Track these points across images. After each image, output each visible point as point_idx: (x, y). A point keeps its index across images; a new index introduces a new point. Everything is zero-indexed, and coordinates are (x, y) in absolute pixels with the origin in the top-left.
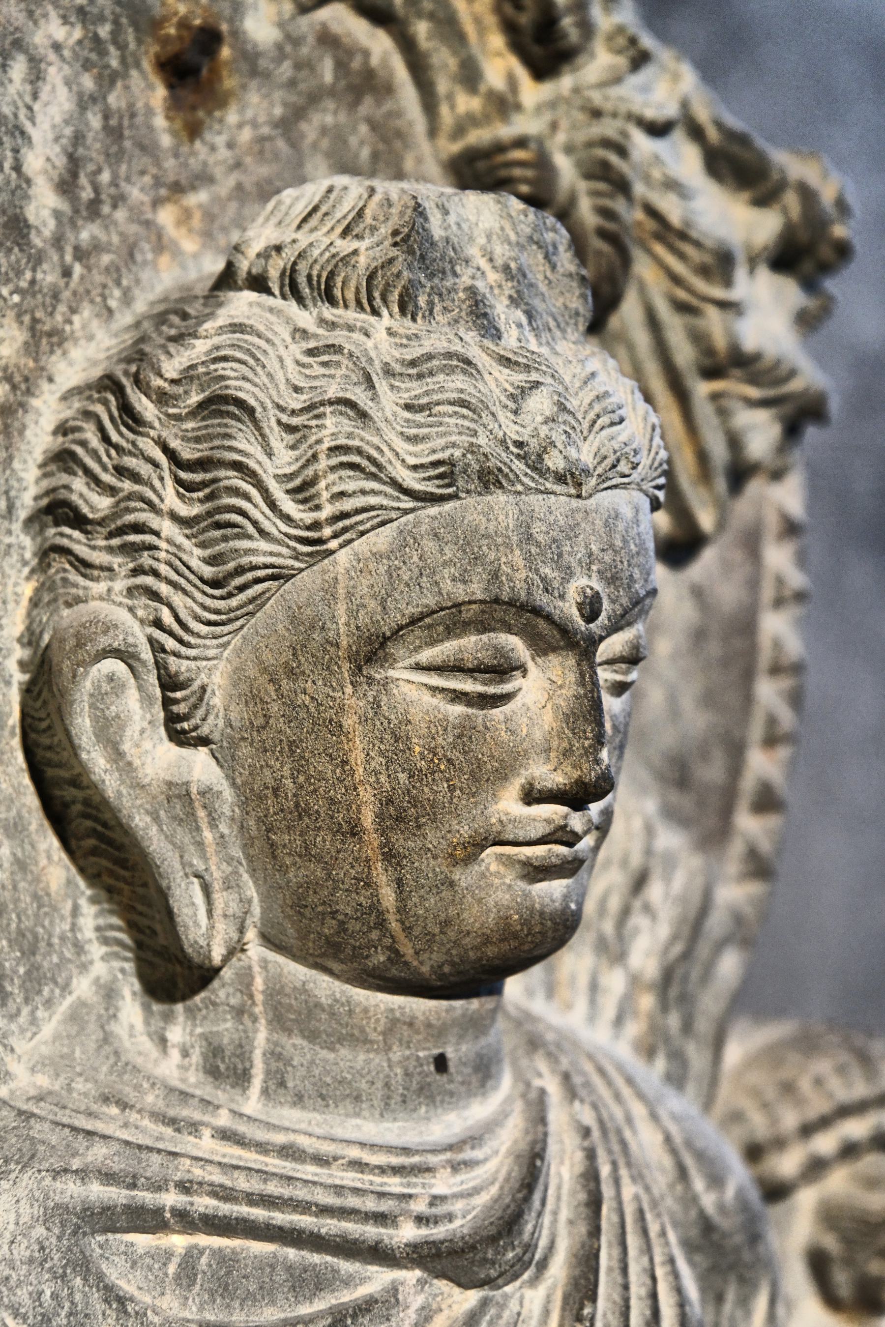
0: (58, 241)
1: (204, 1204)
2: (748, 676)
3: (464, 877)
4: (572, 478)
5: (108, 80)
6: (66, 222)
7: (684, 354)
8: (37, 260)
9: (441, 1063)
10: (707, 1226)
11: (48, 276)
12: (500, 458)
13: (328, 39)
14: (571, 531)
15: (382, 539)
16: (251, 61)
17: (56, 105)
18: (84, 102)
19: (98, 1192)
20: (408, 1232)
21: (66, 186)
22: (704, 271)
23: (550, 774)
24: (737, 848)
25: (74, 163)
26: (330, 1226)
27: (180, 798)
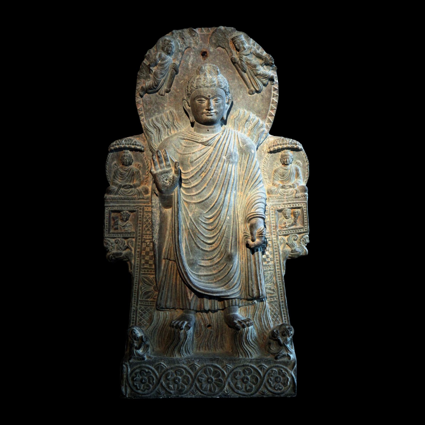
0: (191, 69)
1: (188, 138)
2: (269, 103)
3: (203, 116)
4: (207, 87)
5: (196, 56)
6: (192, 68)
7: (253, 75)
8: (189, 71)
9: (208, 130)
10: (241, 148)
11: (190, 72)
12: (201, 86)
13: (218, 50)
14: (208, 91)
15: (194, 91)
16: (211, 53)
17: (192, 59)
18: (194, 58)
19: (182, 137)
20: (200, 141)
21: (192, 65)
22: (253, 67)
23: (207, 108)
24: (267, 119)
25: (193, 63)
26: (195, 140)
27: (189, 110)
